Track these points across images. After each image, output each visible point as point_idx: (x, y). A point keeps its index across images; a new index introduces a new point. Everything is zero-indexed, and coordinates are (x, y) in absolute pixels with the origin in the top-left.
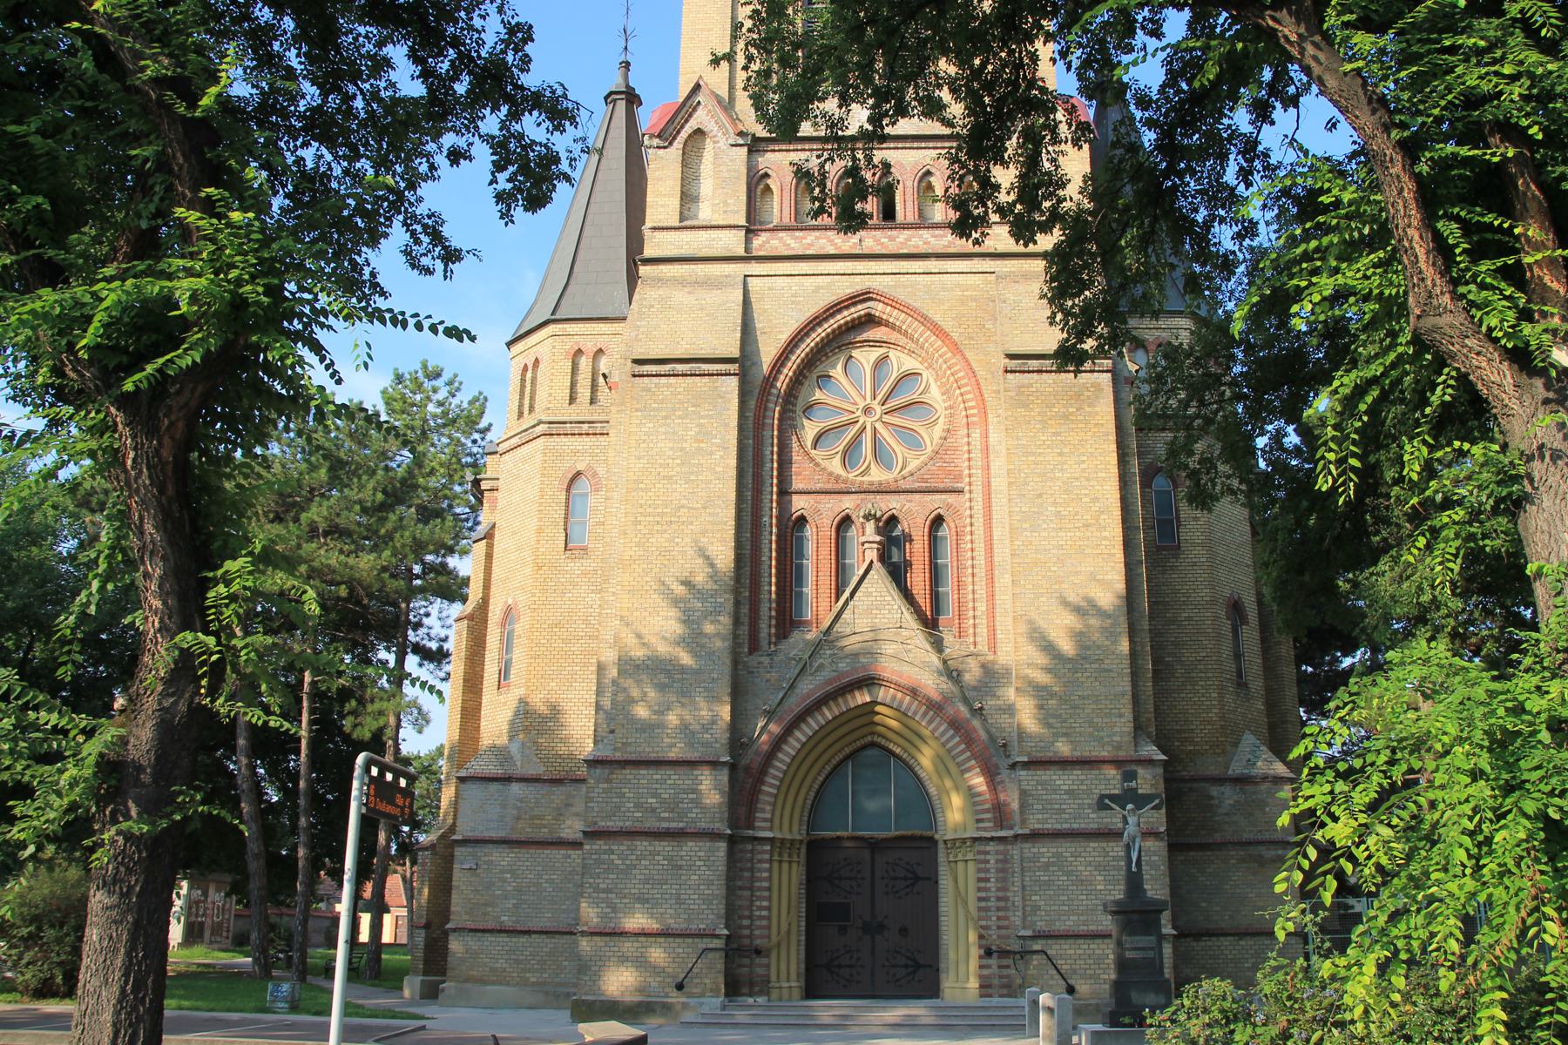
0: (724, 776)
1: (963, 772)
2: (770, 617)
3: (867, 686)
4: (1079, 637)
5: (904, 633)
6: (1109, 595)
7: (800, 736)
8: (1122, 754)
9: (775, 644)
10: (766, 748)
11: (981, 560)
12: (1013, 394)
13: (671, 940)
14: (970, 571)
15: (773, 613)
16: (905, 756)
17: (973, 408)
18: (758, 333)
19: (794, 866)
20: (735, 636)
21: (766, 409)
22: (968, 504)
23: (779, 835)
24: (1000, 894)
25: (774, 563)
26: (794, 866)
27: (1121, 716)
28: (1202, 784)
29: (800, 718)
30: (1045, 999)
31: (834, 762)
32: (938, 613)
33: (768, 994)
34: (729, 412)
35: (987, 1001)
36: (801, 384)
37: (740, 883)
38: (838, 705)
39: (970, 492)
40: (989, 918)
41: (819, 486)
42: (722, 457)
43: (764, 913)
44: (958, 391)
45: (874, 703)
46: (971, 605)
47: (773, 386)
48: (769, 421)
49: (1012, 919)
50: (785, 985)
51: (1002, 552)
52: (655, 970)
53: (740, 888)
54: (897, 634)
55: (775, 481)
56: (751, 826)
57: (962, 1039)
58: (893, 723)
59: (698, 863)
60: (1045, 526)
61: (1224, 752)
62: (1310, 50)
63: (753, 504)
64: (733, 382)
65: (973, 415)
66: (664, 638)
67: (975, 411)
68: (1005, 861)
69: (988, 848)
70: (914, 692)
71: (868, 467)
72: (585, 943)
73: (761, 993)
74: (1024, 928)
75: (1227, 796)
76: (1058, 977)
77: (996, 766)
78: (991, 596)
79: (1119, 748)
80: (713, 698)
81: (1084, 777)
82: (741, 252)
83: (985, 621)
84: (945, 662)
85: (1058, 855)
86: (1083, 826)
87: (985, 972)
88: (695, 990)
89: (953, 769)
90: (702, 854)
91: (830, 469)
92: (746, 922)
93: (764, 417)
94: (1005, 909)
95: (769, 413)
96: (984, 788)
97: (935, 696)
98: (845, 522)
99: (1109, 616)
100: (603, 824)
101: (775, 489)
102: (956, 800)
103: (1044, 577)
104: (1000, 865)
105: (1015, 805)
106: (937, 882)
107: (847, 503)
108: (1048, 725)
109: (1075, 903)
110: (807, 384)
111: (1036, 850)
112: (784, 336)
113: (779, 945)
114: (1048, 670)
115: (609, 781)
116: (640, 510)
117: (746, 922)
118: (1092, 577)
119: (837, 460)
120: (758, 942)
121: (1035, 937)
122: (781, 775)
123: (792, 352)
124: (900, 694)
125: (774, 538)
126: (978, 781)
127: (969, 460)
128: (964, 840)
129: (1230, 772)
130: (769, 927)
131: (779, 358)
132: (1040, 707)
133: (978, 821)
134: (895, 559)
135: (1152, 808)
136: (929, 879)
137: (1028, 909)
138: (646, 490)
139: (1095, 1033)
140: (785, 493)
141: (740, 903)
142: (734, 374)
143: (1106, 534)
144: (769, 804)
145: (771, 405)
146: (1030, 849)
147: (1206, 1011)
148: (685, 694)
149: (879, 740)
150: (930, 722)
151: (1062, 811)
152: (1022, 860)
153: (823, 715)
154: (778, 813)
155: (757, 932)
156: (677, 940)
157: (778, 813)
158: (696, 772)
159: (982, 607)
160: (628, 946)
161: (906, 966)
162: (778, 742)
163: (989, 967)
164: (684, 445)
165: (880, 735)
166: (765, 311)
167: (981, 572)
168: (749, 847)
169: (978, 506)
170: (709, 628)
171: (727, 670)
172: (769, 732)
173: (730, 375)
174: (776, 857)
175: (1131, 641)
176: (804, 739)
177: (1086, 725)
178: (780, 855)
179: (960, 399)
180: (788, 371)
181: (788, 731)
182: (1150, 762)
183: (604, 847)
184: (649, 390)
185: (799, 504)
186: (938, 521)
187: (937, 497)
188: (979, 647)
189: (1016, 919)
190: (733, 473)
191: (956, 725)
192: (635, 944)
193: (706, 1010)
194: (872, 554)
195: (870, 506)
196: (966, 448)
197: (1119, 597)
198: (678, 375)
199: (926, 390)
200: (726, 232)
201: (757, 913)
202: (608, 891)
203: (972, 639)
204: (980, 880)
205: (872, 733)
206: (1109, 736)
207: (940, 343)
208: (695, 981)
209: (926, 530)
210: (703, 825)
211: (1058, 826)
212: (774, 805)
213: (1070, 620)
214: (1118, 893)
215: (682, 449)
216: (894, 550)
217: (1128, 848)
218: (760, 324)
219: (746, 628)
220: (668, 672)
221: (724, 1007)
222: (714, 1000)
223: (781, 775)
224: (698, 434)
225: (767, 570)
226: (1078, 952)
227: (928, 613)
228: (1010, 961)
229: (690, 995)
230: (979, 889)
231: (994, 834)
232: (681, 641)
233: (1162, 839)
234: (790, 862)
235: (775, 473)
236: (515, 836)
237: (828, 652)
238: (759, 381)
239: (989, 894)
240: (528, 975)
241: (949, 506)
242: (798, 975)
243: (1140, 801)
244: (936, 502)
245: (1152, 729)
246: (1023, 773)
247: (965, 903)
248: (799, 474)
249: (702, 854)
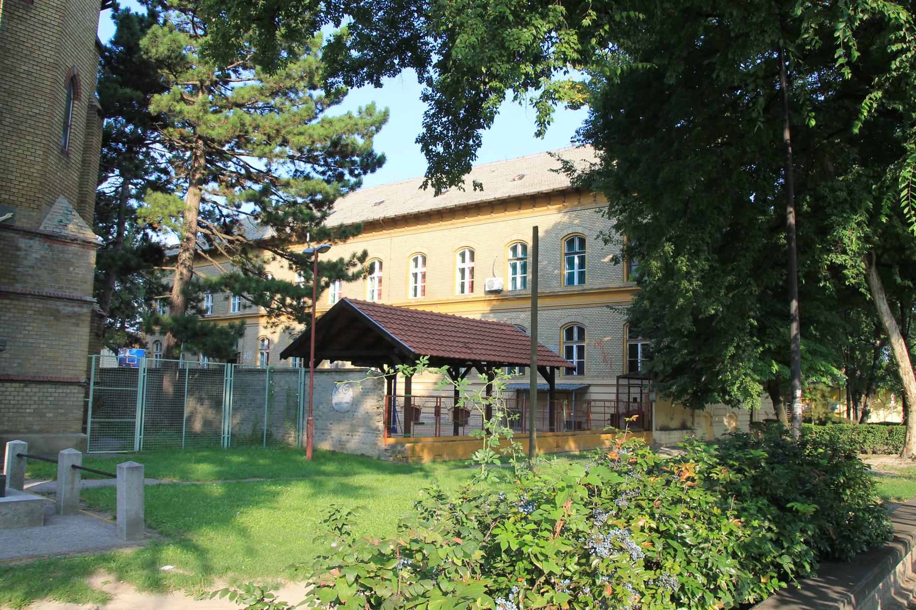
61: (39, 207)
75: (35, 250)
129: (42, 228)
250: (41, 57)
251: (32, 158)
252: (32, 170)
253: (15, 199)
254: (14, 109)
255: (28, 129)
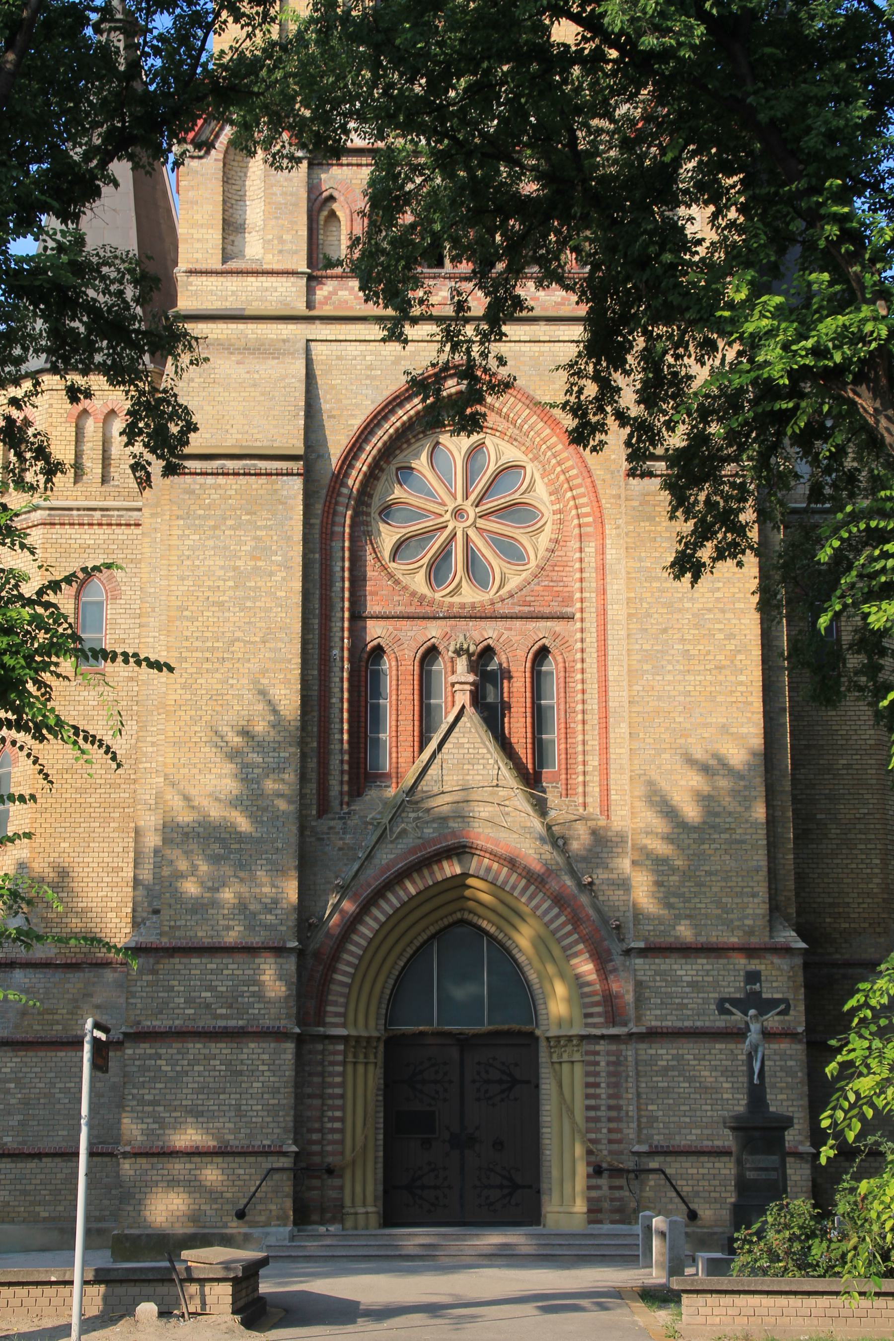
0: (291, 964)
1: (568, 958)
2: (342, 772)
3: (458, 855)
4: (706, 800)
5: (502, 793)
6: (743, 751)
7: (379, 914)
8: (755, 941)
9: (348, 804)
10: (337, 931)
11: (593, 705)
12: (636, 503)
13: (231, 1159)
14: (580, 717)
15: (346, 767)
16: (501, 936)
17: (587, 515)
18: (325, 417)
19: (371, 1068)
20: (302, 796)
21: (335, 513)
22: (579, 635)
23: (353, 1033)
24: (612, 1102)
25: (346, 706)
26: (371, 1068)
27: (754, 895)
28: (860, 971)
29: (379, 894)
30: (658, 1222)
31: (417, 943)
32: (541, 766)
33: (342, 1221)
34: (293, 523)
35: (596, 1229)
36: (377, 478)
37: (309, 1090)
38: (423, 877)
39: (582, 620)
40: (598, 1130)
41: (399, 609)
42: (284, 579)
43: (337, 1125)
44: (569, 494)
45: (465, 875)
46: (580, 758)
47: (343, 484)
48: (339, 529)
49: (626, 1131)
50: (361, 1210)
51: (618, 696)
52: (213, 1195)
53: (310, 1096)
54: (492, 794)
55: (347, 604)
56: (321, 1023)
57: (568, 1268)
58: (486, 898)
59: (261, 1068)
60: (670, 667)
62: (884, 422)
63: (321, 634)
64: (296, 485)
65: (588, 525)
66: (217, 799)
67: (590, 519)
68: (617, 1062)
69: (598, 1048)
70: (512, 863)
71: (459, 585)
72: (127, 1166)
73: (332, 1221)
74: (639, 1142)
76: (677, 1200)
77: (608, 952)
78: (605, 749)
79: (751, 933)
80: (277, 870)
81: (709, 967)
82: (300, 307)
83: (597, 779)
84: (549, 828)
85: (679, 1058)
86: (707, 1024)
87: (594, 1194)
88: (258, 1218)
89: (557, 951)
90: (266, 1057)
91: (413, 587)
92: (315, 1137)
93: (333, 524)
94: (618, 1119)
95: (338, 519)
96: (593, 977)
97: (537, 867)
98: (431, 654)
99: (742, 777)
100: (148, 1024)
101: (347, 615)
102: (560, 989)
103: (667, 729)
104: (611, 1068)
105: (630, 997)
106: (537, 1086)
107: (434, 631)
108: (669, 906)
109: (698, 1113)
110: (384, 477)
111: (653, 1052)
112: (357, 422)
113: (354, 1162)
114: (668, 839)
115: (154, 972)
116: (188, 644)
117: (315, 1137)
118: (724, 729)
119: (421, 576)
120: (330, 1159)
121: (652, 1153)
122: (356, 961)
123: (366, 441)
124: (495, 866)
125: (346, 675)
126: (586, 967)
127: (581, 580)
128: (570, 1038)
130: (342, 1142)
131: (351, 449)
132: (658, 884)
133: (587, 1015)
134: (490, 699)
135: (779, 1014)
136: (528, 1082)
137: (644, 1120)
138: (193, 619)
139: (711, 1261)
140: (358, 617)
141: (309, 1114)
142: (298, 474)
143: (742, 678)
144: (341, 995)
145: (341, 509)
146: (648, 1050)
147: (787, 1227)
148: (243, 865)
149: (467, 916)
150: (531, 898)
151: (682, 1006)
152: (637, 1064)
153: (405, 890)
154: (352, 1006)
155: (329, 1148)
156: (238, 1159)
157: (352, 1006)
158: (257, 961)
159: (593, 761)
160: (178, 1167)
161: (501, 1187)
162: (352, 924)
163: (598, 1187)
164: (238, 563)
165: (471, 912)
166: (333, 387)
167: (593, 719)
168: (320, 1047)
169: (591, 638)
170: (270, 785)
171: (294, 839)
172: (342, 912)
173: (292, 474)
174: (350, 1059)
175: (769, 805)
176: (383, 918)
177: (713, 906)
178: (355, 1056)
179: (572, 503)
180: (362, 465)
181: (364, 909)
182: (786, 951)
183: (149, 1051)
184: (193, 492)
185: (375, 631)
186: (542, 653)
187: (542, 624)
188: (590, 809)
189: (630, 1131)
190: (298, 599)
191: (559, 900)
192: (188, 1166)
193: (272, 1241)
194: (463, 698)
195: (461, 638)
196: (577, 565)
197: (754, 754)
198: (228, 474)
199: (531, 488)
200: (283, 279)
201: (329, 1125)
202: (154, 1103)
203: (581, 800)
204: (588, 1085)
205: (462, 909)
206: (739, 919)
207: (548, 431)
208: (259, 1207)
209: (528, 665)
210: (267, 1023)
211: (679, 1024)
212: (347, 997)
213: (695, 780)
214: (740, 1104)
215: (235, 568)
216: (490, 688)
217: (750, 1057)
218: (326, 404)
219: (314, 786)
220: (222, 841)
221: (292, 1238)
222: (281, 1229)
223: (356, 961)
224: (255, 548)
225: (337, 714)
226: (701, 1171)
227: (530, 766)
228: (622, 1182)
229: (253, 1224)
230: (588, 1096)
231: (605, 1031)
232: (236, 803)
233: (800, 1042)
234: (366, 1064)
235: (347, 595)
236: (19, 1036)
237: (412, 815)
238: (326, 480)
239: (599, 1102)
240: (37, 1209)
241: (556, 636)
242: (376, 1198)
243: (765, 1006)
244: (540, 631)
245: (792, 910)
246: (639, 961)
247: (571, 1112)
248: (375, 593)
249: (266, 1057)
250: (859, 742)
251: (869, 871)
252: (870, 886)
253: (856, 926)
254: (839, 817)
255: (859, 836)
